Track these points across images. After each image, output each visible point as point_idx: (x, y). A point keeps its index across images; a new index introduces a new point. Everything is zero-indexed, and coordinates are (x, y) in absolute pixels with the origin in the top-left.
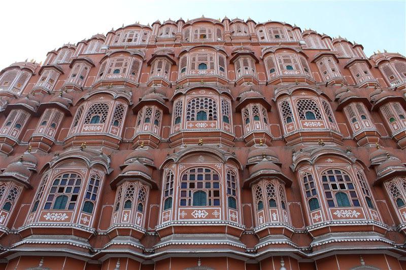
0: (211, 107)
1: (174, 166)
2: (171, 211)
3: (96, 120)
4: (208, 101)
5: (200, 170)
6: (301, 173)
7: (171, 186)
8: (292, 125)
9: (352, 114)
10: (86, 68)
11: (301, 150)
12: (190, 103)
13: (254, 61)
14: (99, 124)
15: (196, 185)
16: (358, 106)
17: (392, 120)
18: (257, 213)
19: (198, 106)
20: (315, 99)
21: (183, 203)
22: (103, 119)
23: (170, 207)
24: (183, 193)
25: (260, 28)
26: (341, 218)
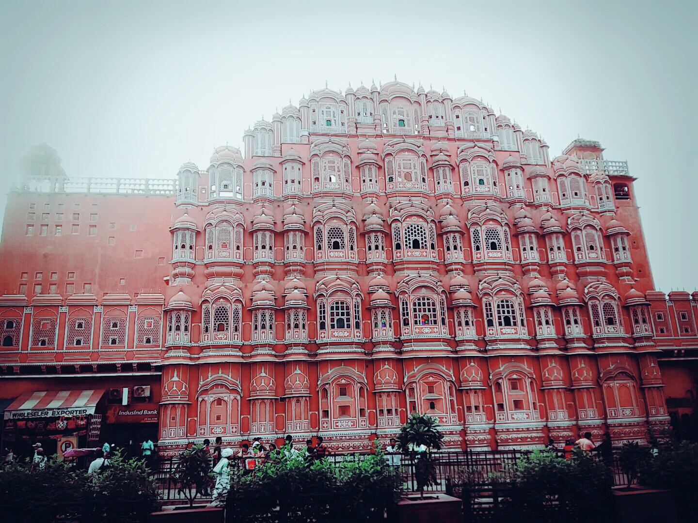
0: (422, 236)
1: (406, 295)
2: (409, 327)
3: (336, 246)
4: (419, 228)
5: (424, 299)
6: (484, 300)
7: (407, 310)
8: (480, 253)
9: (524, 244)
10: (299, 169)
11: (485, 282)
12: (406, 230)
13: (451, 168)
14: (340, 250)
15: (422, 310)
16: (530, 237)
17: (552, 249)
18: (457, 328)
19: (412, 234)
20: (499, 228)
21: (416, 322)
22: (342, 245)
23: (408, 324)
24: (415, 316)
25: (457, 112)
26: (505, 334)
